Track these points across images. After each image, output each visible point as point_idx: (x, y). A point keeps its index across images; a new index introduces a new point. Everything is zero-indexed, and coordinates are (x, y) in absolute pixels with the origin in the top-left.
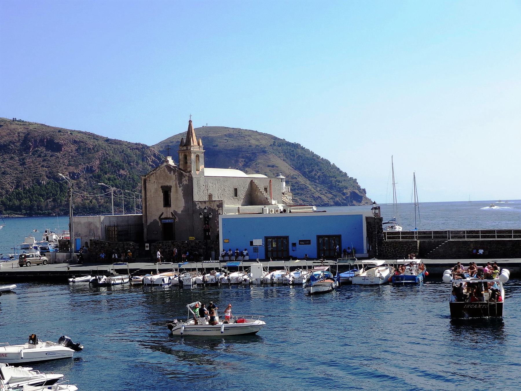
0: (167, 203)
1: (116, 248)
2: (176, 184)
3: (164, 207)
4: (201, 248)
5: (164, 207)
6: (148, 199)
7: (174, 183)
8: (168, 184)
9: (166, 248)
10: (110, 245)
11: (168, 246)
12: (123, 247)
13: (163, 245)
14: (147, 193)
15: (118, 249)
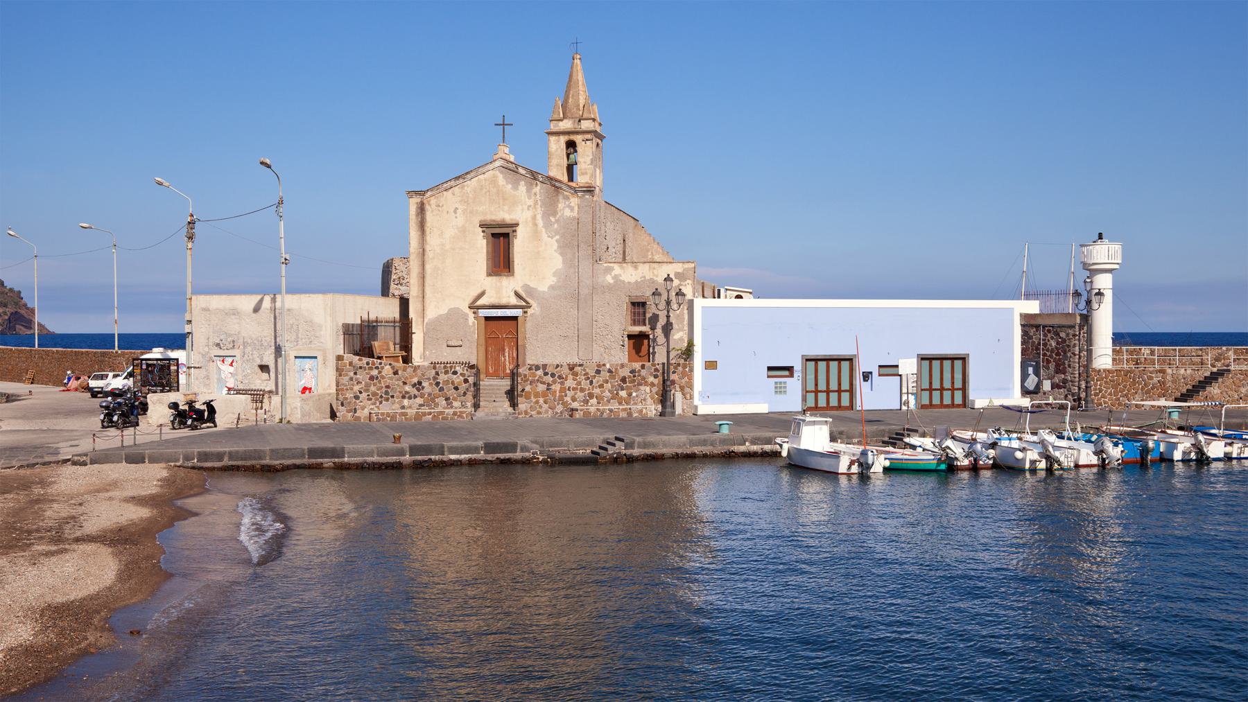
0: (501, 262)
1: (415, 380)
2: (534, 218)
3: (489, 275)
4: (646, 384)
5: (489, 275)
6: (429, 254)
7: (529, 214)
8: (508, 218)
9: (554, 382)
10: (396, 373)
11: (560, 377)
12: (435, 378)
13: (546, 374)
14: (428, 238)
15: (420, 383)
